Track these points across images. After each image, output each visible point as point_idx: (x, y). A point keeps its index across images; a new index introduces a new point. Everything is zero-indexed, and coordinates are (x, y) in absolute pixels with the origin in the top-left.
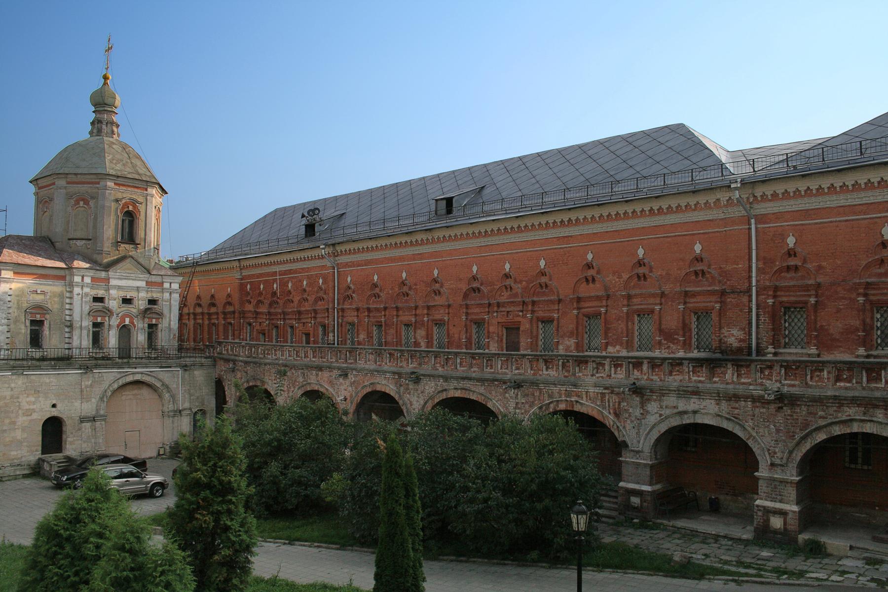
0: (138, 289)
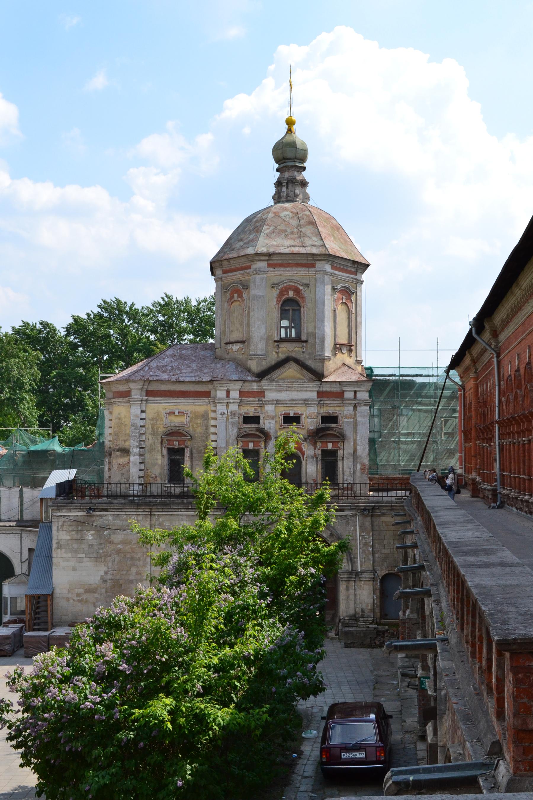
0: (306, 402)
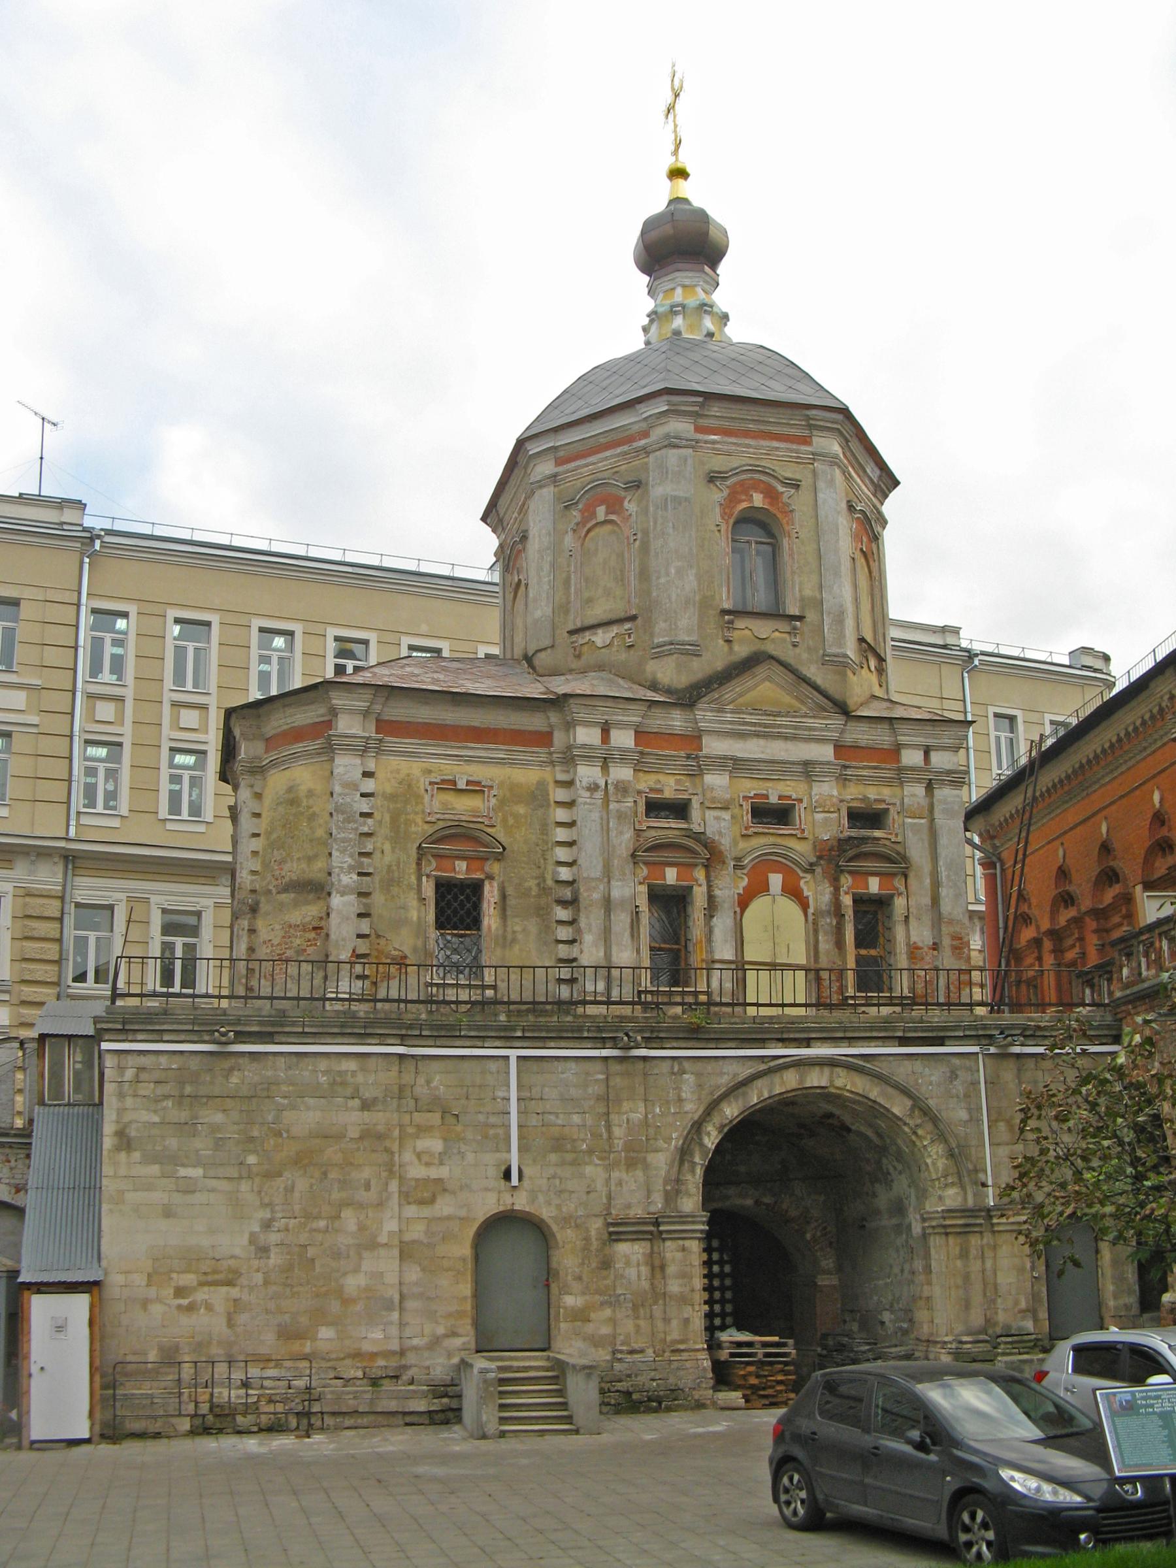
0: (808, 770)
